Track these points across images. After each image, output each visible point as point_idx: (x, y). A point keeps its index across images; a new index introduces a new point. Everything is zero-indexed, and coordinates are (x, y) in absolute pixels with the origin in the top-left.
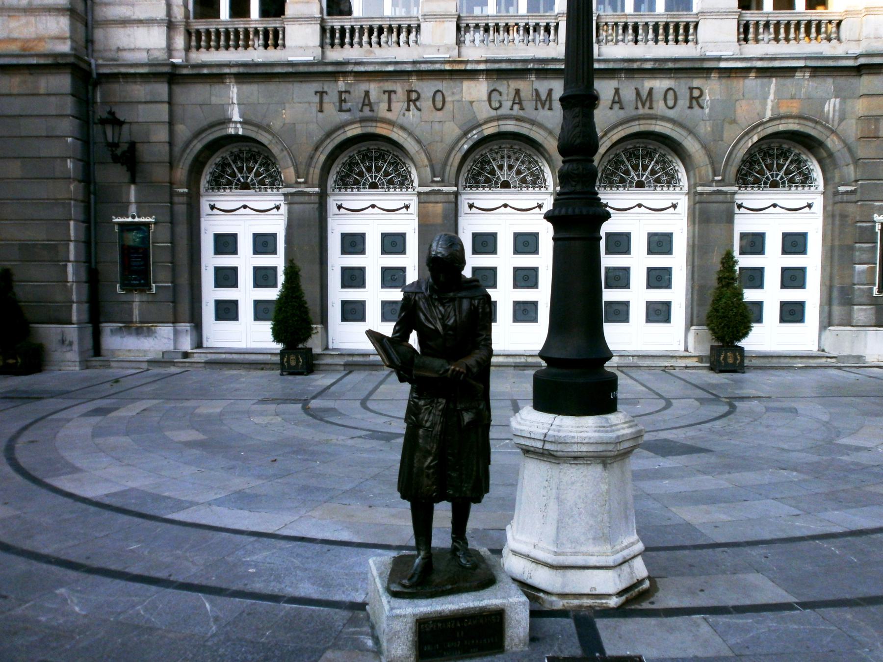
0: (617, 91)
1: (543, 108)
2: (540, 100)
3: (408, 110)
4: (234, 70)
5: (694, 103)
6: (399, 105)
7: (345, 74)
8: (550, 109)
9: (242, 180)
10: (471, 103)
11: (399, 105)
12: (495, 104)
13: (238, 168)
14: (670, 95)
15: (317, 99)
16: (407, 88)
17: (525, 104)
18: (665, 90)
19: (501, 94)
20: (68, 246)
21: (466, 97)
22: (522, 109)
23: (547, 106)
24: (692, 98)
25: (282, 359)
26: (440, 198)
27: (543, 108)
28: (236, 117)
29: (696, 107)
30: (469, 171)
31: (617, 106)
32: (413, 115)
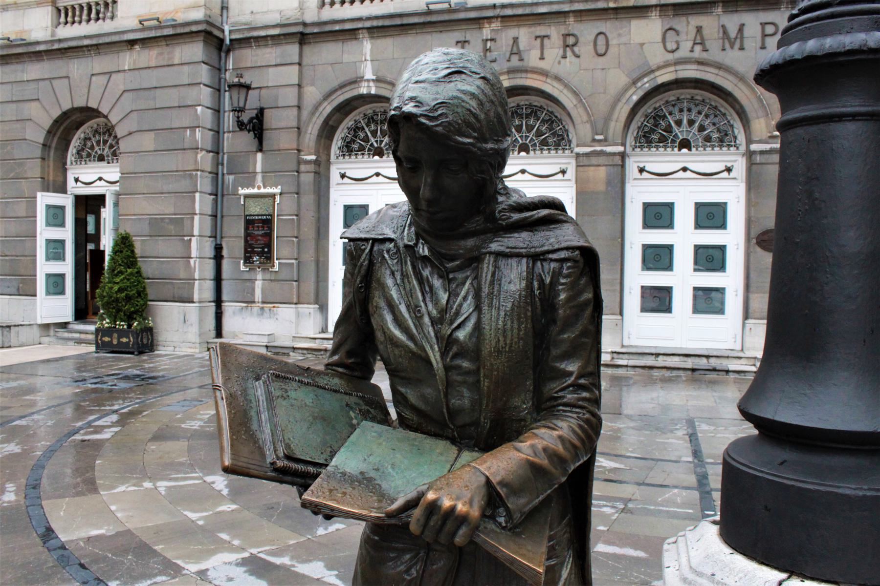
1: (732, 47)
2: (728, 38)
3: (564, 57)
4: (368, 24)
7: (489, 19)
8: (742, 48)
10: (642, 45)
11: (553, 51)
12: (671, 46)
13: (372, 132)
16: (563, 31)
17: (708, 44)
19: (677, 33)
20: (193, 219)
22: (705, 50)
26: (602, 160)
27: (732, 47)
28: (369, 75)
30: (639, 128)
32: (571, 63)
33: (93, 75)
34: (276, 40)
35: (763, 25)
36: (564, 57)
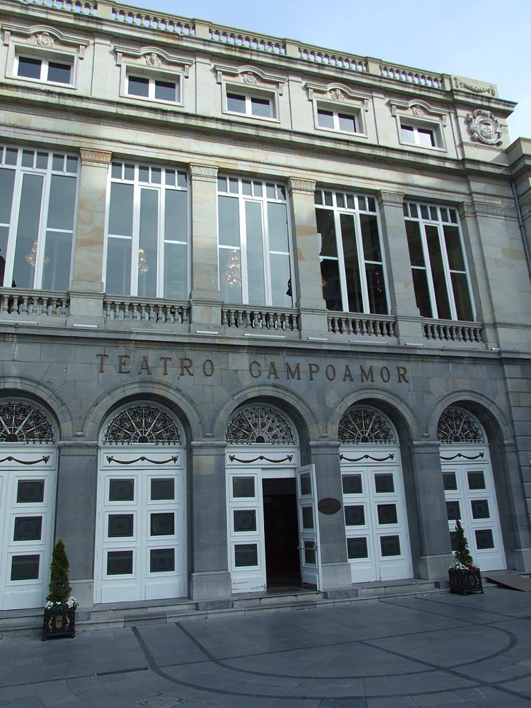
5: (401, 377)
9: (9, 433)
11: (174, 371)
14: (385, 371)
15: (98, 361)
16: (183, 357)
18: (381, 368)
21: (233, 367)
23: (296, 377)
24: (400, 375)
25: (46, 621)
29: (403, 382)
31: (348, 379)
36: (182, 374)
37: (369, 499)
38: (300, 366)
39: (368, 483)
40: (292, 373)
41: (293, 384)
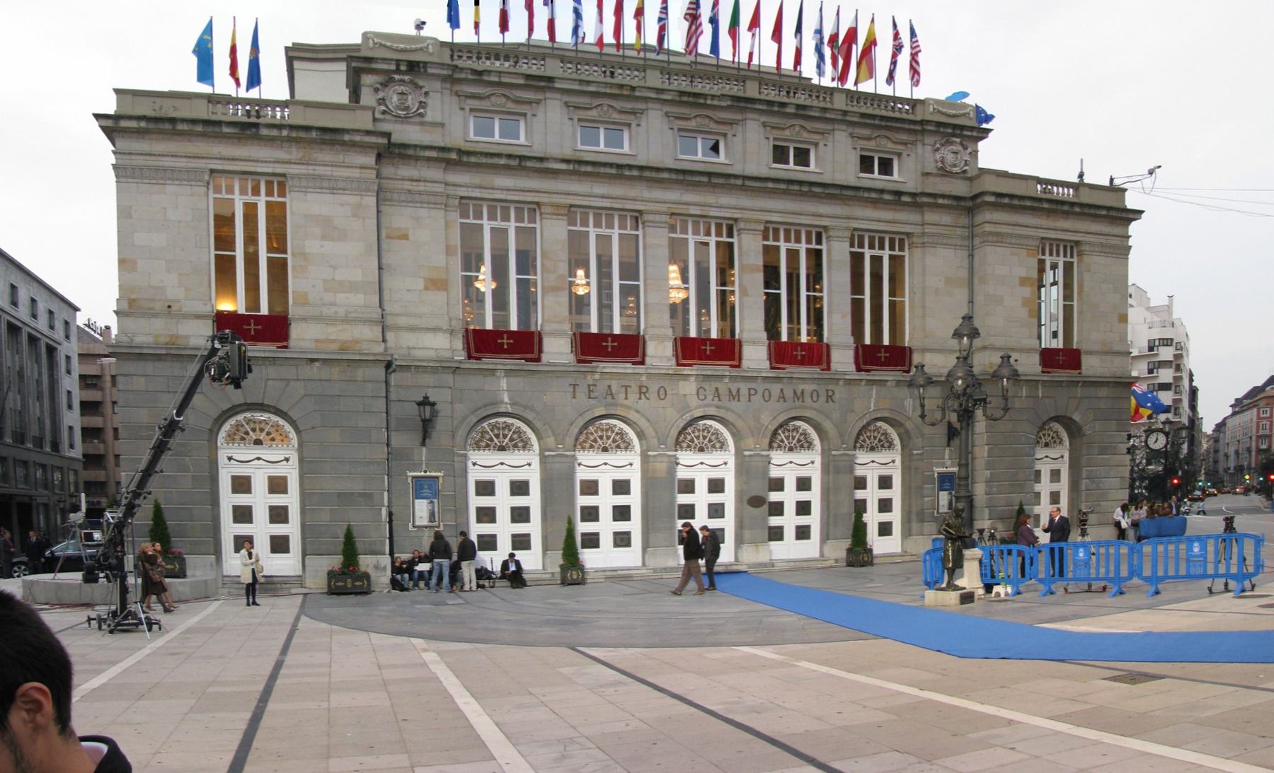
0: (782, 390)
1: (734, 399)
3: (640, 398)
6: (633, 396)
8: (739, 400)
10: (685, 395)
11: (633, 396)
17: (722, 398)
19: (705, 390)
21: (682, 392)
23: (736, 399)
24: (827, 396)
27: (734, 399)
28: (506, 399)
29: (830, 402)
33: (268, 379)
34: (434, 370)
35: (749, 389)
37: (789, 497)
38: (741, 391)
39: (790, 484)
40: (734, 396)
41: (734, 405)
